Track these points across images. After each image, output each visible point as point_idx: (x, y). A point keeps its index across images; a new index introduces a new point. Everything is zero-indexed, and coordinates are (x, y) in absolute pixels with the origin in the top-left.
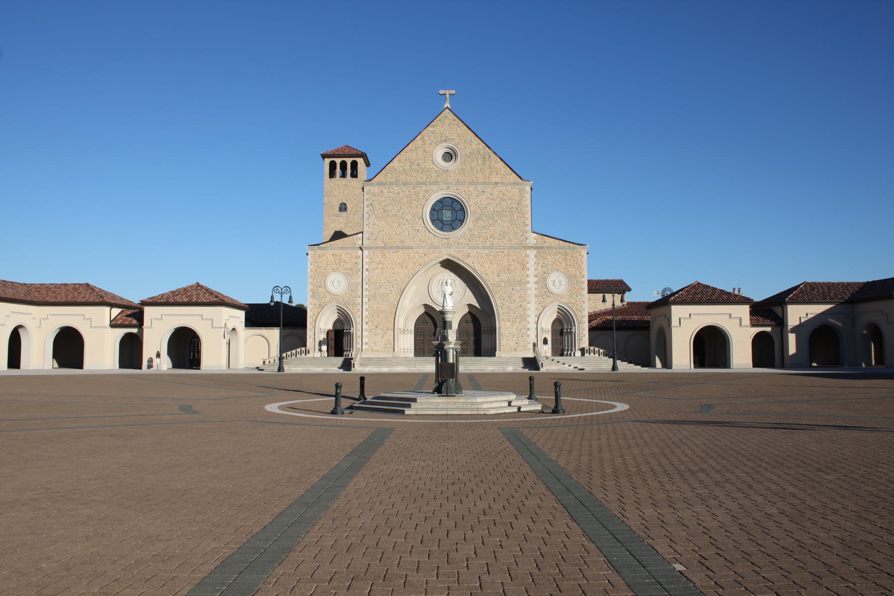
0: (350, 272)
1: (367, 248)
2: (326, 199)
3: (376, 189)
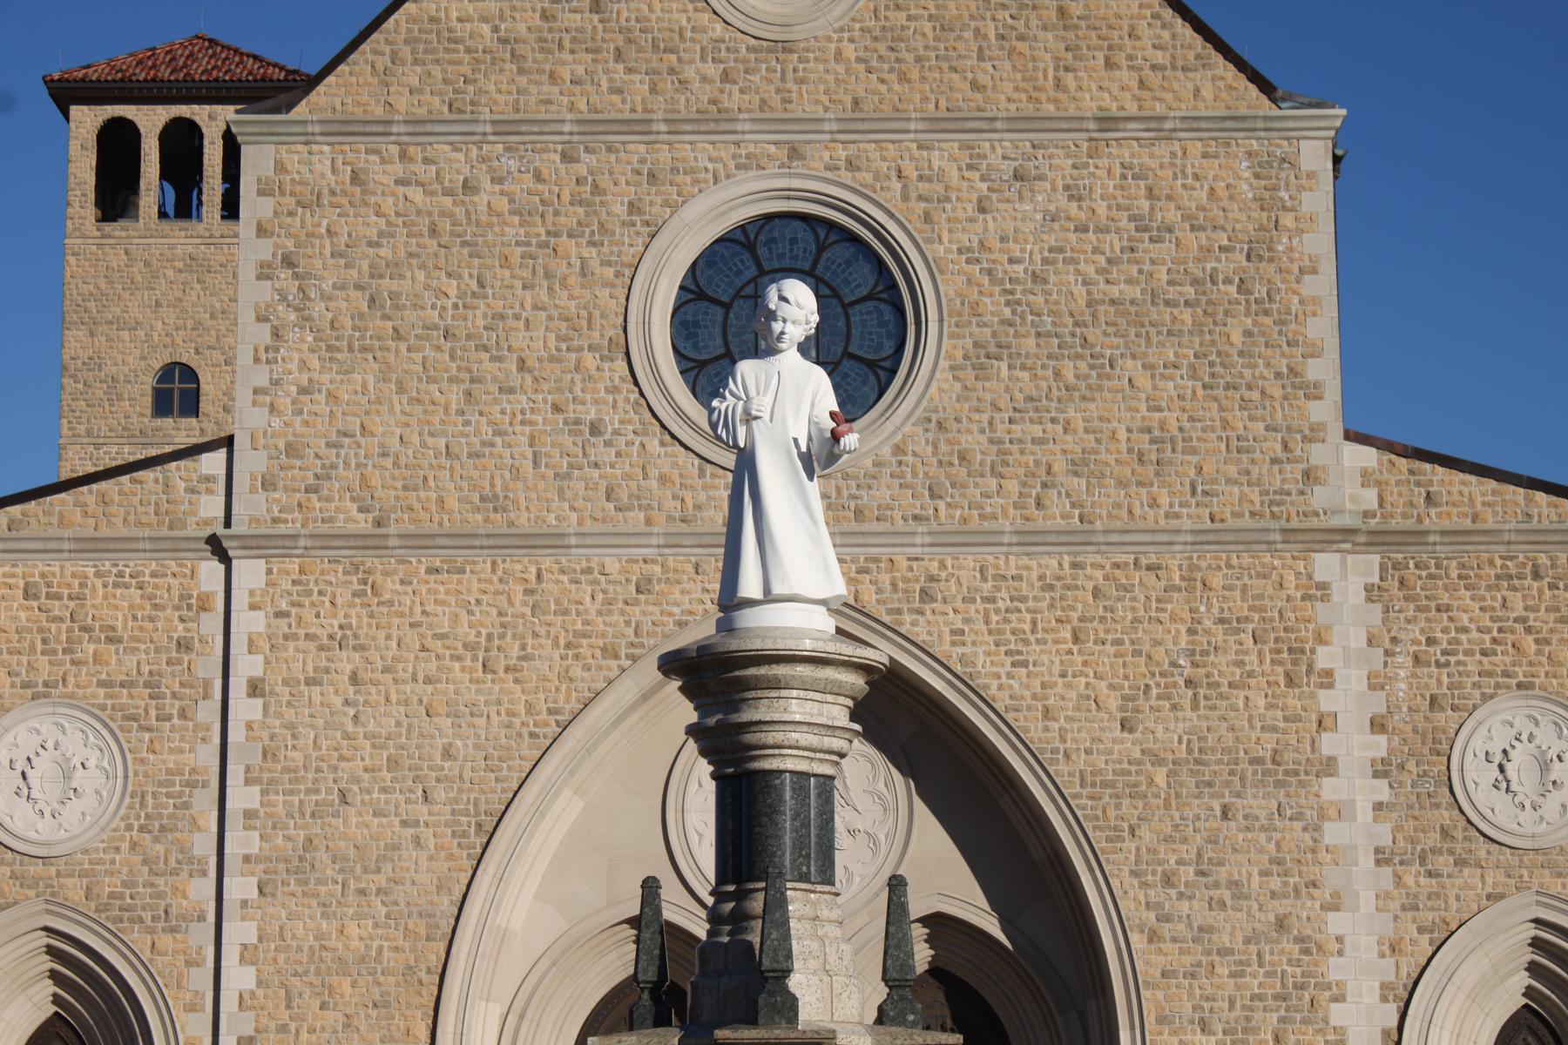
0: (139, 700)
1: (258, 545)
2: (76, 343)
3: (319, 164)
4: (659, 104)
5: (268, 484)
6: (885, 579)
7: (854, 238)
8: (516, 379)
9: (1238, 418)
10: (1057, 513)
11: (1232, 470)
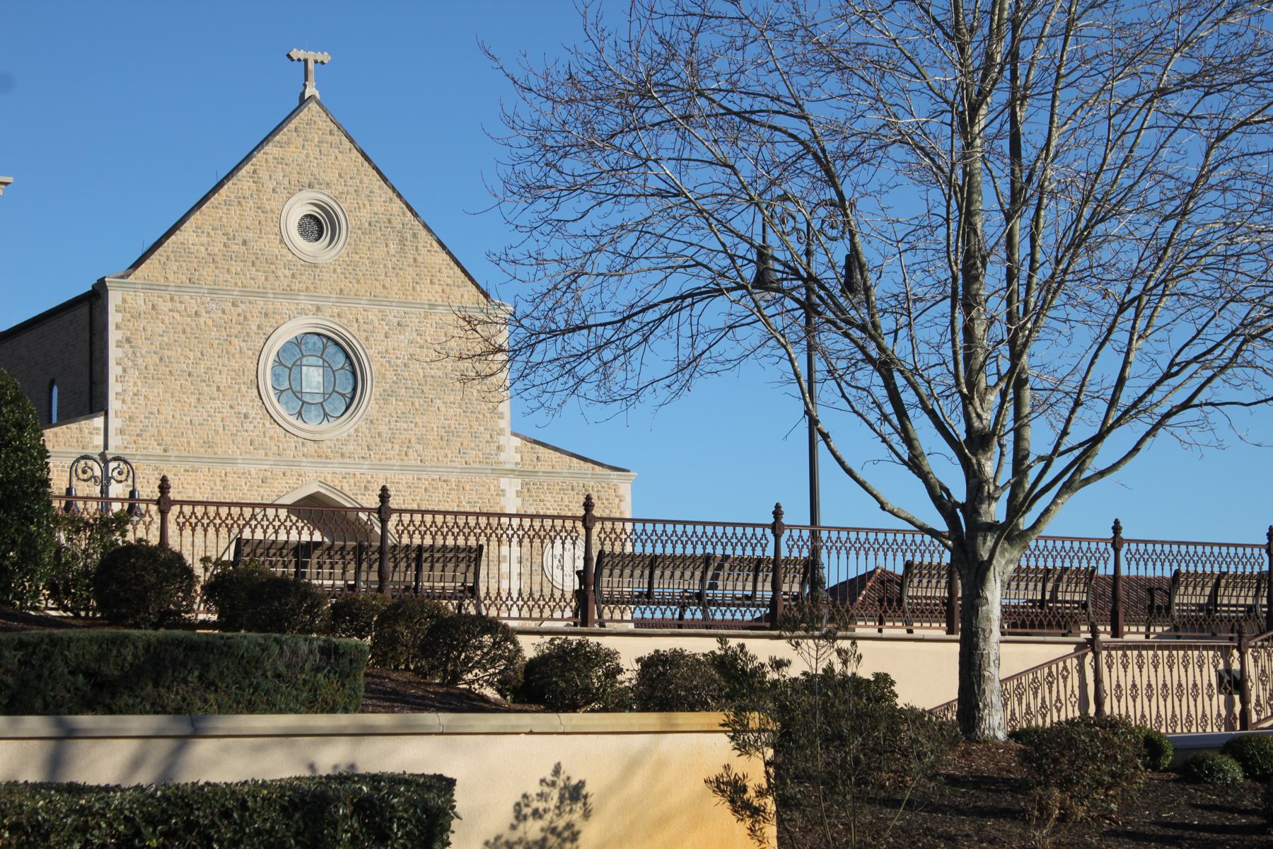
4: (268, 285)
5: (122, 432)
6: (352, 481)
7: (337, 344)
8: (216, 394)
9: (475, 424)
10: (413, 460)
11: (473, 445)
